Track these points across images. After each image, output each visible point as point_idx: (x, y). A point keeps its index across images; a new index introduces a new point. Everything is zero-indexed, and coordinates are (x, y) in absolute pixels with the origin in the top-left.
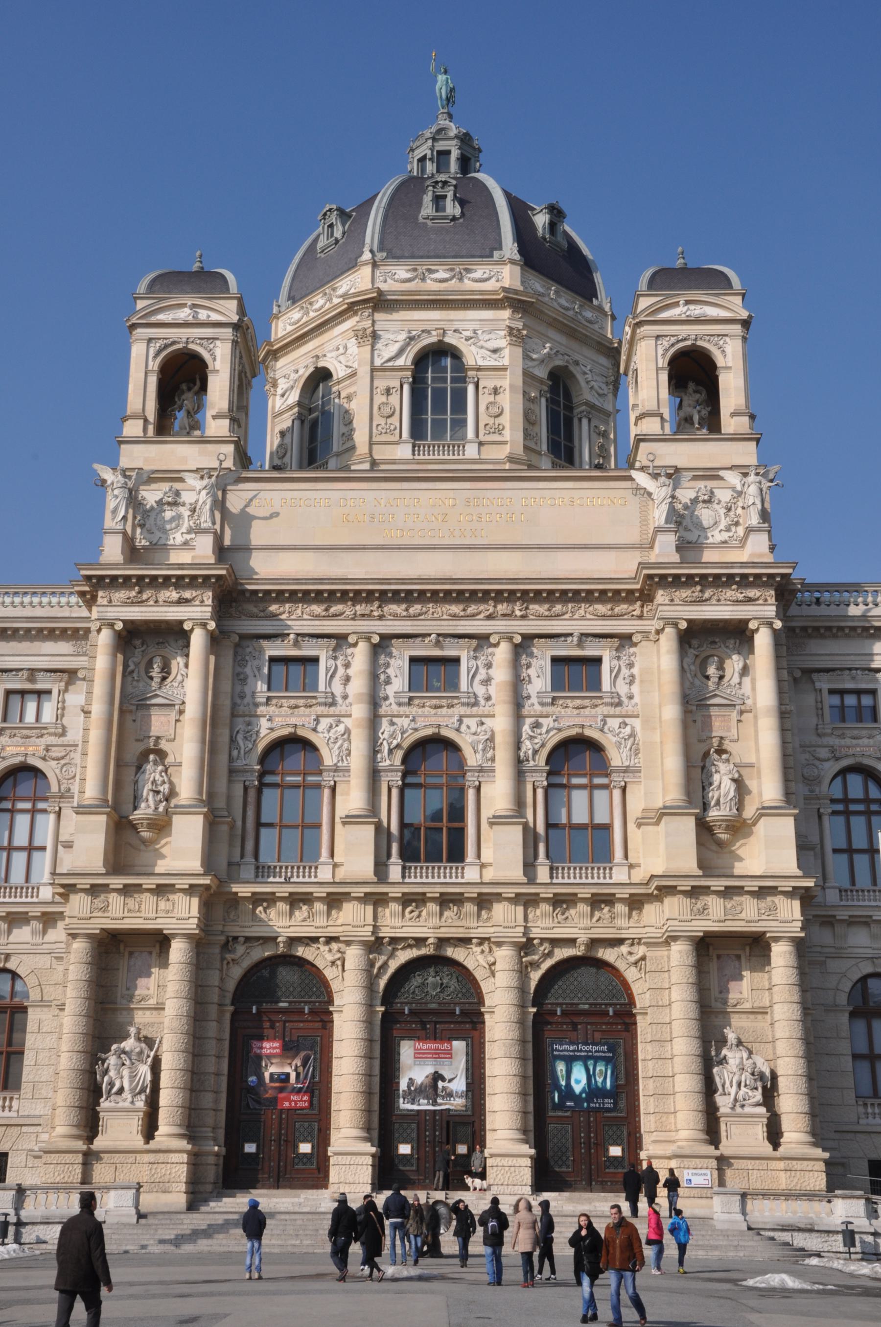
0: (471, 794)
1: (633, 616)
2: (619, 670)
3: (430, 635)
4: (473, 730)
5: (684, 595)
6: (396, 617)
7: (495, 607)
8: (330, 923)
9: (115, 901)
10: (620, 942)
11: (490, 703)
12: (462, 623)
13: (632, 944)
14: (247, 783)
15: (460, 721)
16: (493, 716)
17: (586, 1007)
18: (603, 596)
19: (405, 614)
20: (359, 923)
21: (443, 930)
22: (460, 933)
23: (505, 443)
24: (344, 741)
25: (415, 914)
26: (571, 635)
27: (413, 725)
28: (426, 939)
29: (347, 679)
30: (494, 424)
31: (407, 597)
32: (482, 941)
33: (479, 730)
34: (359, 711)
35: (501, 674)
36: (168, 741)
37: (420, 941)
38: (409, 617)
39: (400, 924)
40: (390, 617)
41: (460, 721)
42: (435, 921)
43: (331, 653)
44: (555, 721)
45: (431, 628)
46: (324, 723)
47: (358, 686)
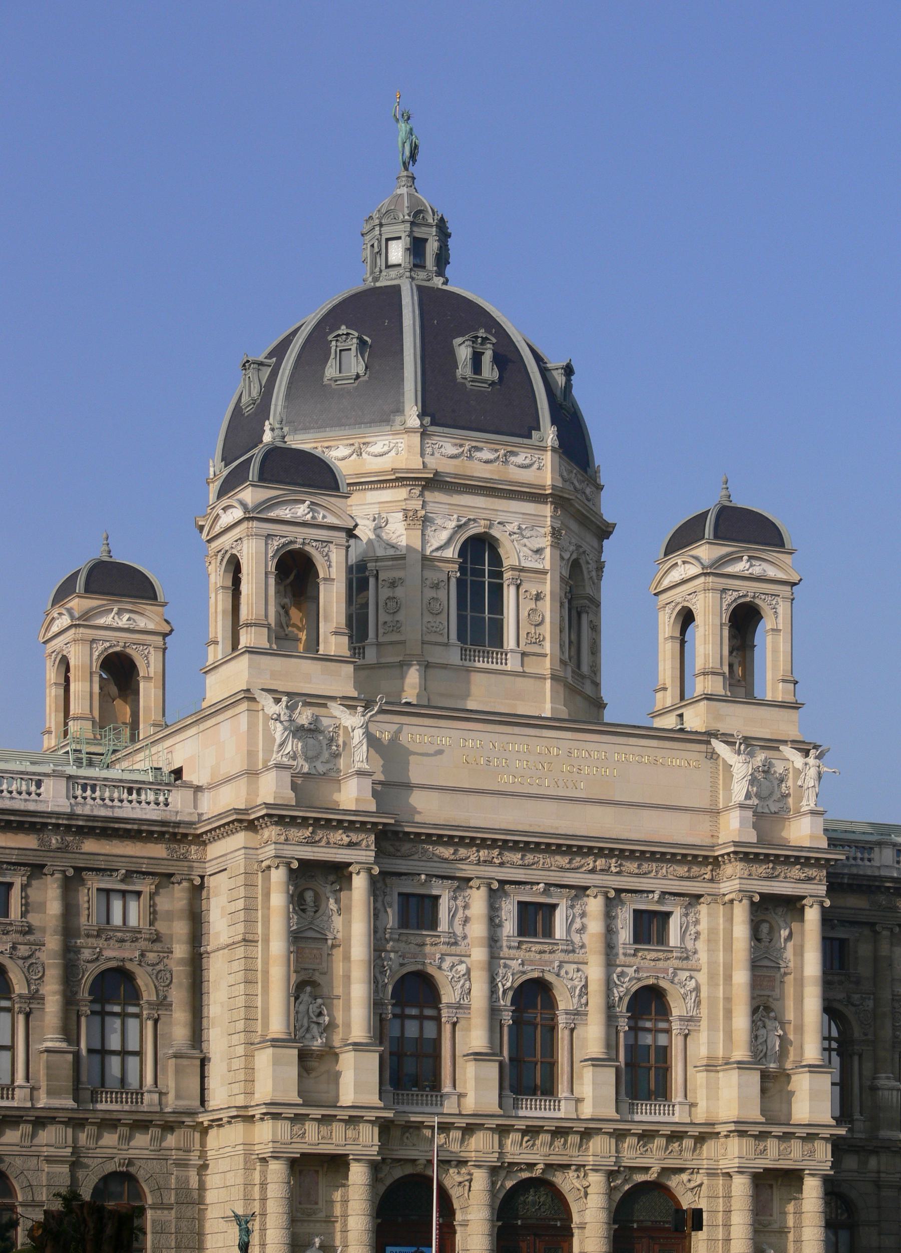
0: (562, 1035)
1: (704, 878)
2: (687, 927)
3: (538, 884)
4: (570, 976)
5: (760, 870)
6: (513, 865)
7: (595, 862)
8: (463, 1149)
9: (311, 1128)
10: (682, 1170)
11: (583, 950)
12: (567, 874)
13: (692, 1173)
14: (383, 1016)
15: (560, 967)
16: (586, 963)
17: (649, 1224)
18: (683, 860)
19: (520, 862)
20: (488, 1150)
21: (552, 1157)
22: (564, 1160)
23: (545, 655)
24: (466, 981)
25: (530, 1143)
26: (653, 892)
27: (521, 968)
28: (535, 1164)
29: (466, 920)
30: (535, 633)
31: (524, 847)
32: (579, 1167)
33: (575, 977)
34: (478, 954)
35: (595, 927)
36: (321, 974)
37: (531, 1166)
38: (523, 866)
39: (518, 1152)
40: (509, 865)
41: (560, 967)
42: (545, 1150)
43: (452, 893)
44: (635, 971)
45: (541, 877)
46: (448, 961)
47: (477, 929)
